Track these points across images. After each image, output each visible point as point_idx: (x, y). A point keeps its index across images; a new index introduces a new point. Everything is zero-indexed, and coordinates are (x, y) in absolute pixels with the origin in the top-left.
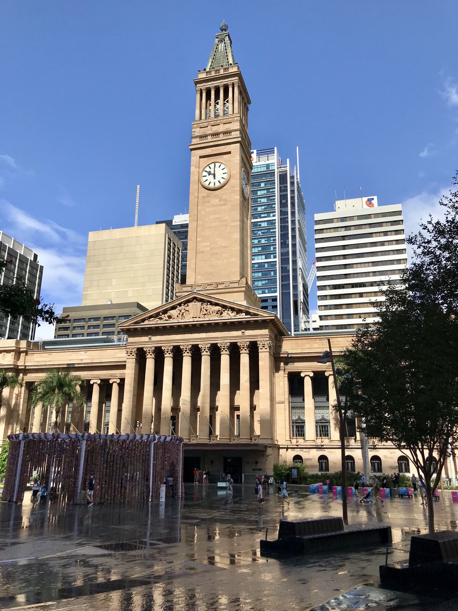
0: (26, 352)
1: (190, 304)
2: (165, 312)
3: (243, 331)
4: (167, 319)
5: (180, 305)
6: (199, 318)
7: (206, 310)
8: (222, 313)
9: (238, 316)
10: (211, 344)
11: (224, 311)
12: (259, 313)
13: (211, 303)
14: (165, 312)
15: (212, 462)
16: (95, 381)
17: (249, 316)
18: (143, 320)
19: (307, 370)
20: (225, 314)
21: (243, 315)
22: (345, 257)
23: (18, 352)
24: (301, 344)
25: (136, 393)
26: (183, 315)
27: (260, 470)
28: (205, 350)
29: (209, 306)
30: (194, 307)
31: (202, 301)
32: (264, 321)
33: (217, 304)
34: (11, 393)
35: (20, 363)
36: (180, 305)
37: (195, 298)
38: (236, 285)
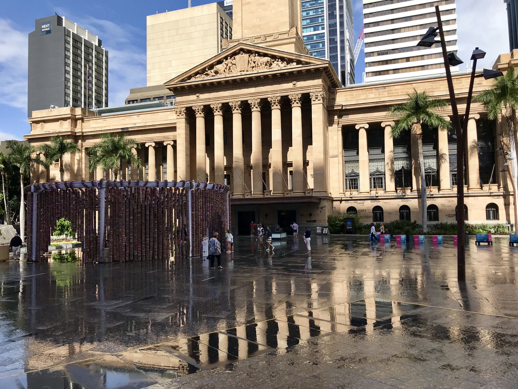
0: (82, 120)
2: (211, 67)
3: (294, 82)
4: (214, 74)
5: (226, 58)
6: (247, 71)
7: (254, 62)
8: (271, 64)
9: (289, 66)
10: (261, 99)
11: (273, 62)
12: (311, 61)
13: (260, 54)
14: (211, 67)
15: (266, 215)
16: (150, 144)
17: (301, 66)
18: (190, 78)
19: (361, 122)
20: (274, 65)
21: (294, 65)
22: (393, 21)
23: (74, 120)
24: (356, 95)
25: (189, 153)
26: (230, 69)
27: (315, 221)
28: (254, 105)
29: (257, 58)
31: (249, 52)
32: (317, 70)
33: (265, 55)
34: (72, 159)
35: (78, 130)
36: (226, 58)
37: (242, 50)
38: (286, 36)
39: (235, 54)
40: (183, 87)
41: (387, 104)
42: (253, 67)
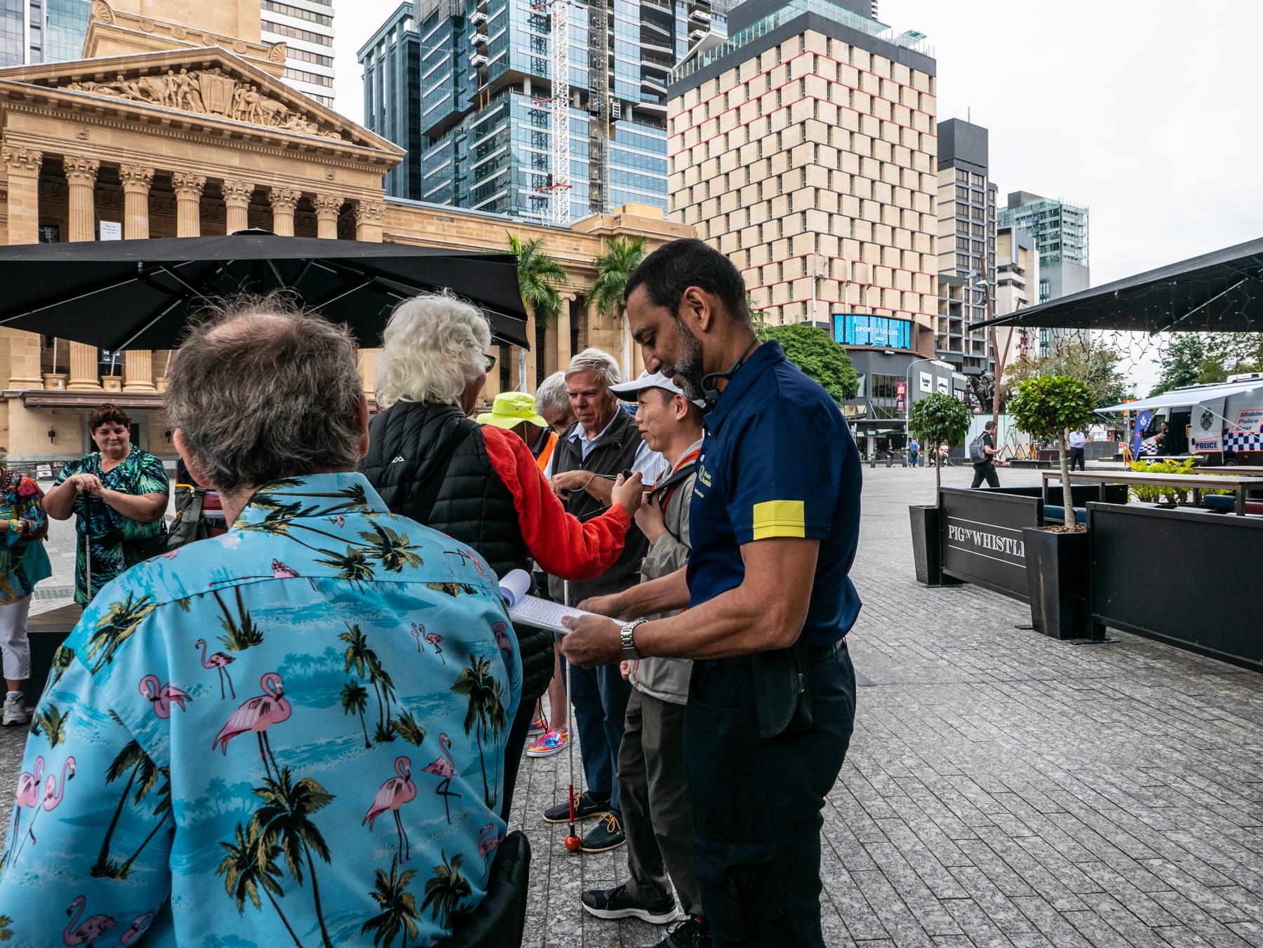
1: (205, 77)
2: (133, 75)
4: (139, 95)
5: (176, 69)
8: (285, 120)
14: (133, 75)
17: (350, 144)
18: (65, 81)
21: (337, 139)
26: (184, 97)
29: (254, 96)
30: (215, 87)
31: (233, 74)
33: (272, 96)
36: (176, 69)
37: (215, 65)
39: (196, 67)
40: (43, 101)
42: (244, 112)
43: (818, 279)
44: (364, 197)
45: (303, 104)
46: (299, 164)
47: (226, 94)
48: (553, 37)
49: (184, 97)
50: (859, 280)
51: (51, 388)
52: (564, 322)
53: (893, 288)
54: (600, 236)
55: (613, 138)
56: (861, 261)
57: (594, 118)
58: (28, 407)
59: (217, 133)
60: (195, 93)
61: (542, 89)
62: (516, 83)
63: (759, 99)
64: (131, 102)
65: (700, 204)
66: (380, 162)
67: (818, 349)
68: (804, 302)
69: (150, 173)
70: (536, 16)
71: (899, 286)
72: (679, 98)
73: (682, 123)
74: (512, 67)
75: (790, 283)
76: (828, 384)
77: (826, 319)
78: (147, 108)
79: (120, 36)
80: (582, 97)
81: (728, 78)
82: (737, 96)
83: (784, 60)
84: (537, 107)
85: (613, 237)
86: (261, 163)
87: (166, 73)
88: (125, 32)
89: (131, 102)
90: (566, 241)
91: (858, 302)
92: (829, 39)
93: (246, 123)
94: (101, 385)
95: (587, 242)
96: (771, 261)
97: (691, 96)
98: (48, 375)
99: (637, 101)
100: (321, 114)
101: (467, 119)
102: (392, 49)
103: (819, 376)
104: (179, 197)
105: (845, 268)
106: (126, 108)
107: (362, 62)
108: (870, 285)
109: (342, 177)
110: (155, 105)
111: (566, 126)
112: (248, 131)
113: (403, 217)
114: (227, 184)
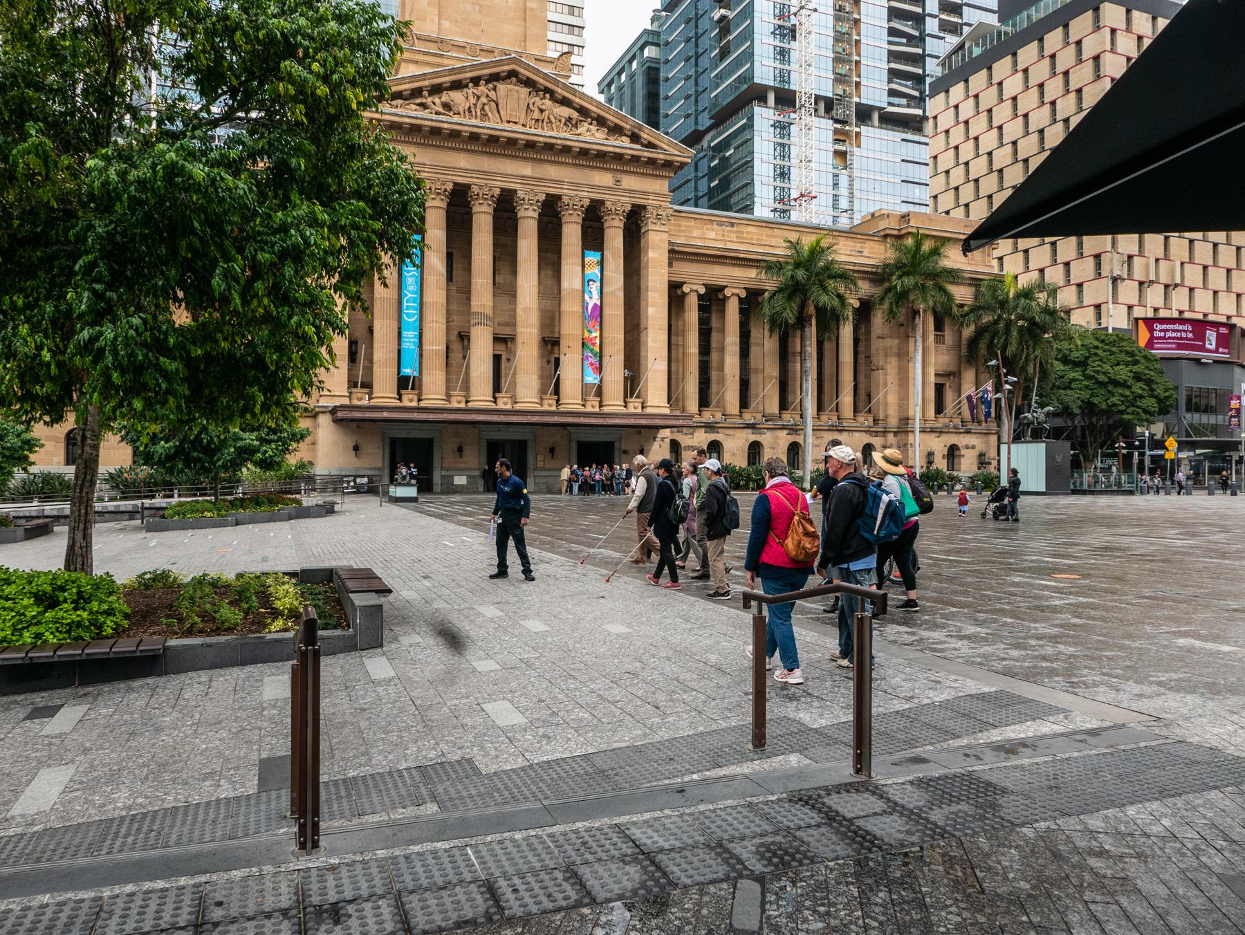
1: (502, 87)
2: (436, 90)
4: (441, 110)
5: (476, 81)
7: (542, 111)
13: (553, 98)
14: (436, 90)
15: (552, 451)
17: (639, 147)
20: (583, 128)
26: (483, 109)
29: (548, 103)
30: (512, 96)
31: (529, 83)
33: (565, 102)
36: (476, 81)
37: (512, 74)
39: (495, 78)
41: (741, 256)
43: (1115, 280)
44: (651, 202)
45: (594, 109)
46: (587, 172)
47: (521, 103)
48: (796, 48)
49: (483, 109)
50: (1164, 279)
51: (356, 402)
52: (846, 332)
53: (1205, 287)
54: (886, 236)
55: (859, 146)
56: (1166, 257)
57: (838, 126)
58: (337, 421)
59: (512, 142)
60: (493, 104)
61: (786, 99)
62: (758, 94)
63: (1041, 86)
64: (434, 117)
65: (967, 205)
66: (668, 164)
67: (1123, 357)
68: (1098, 307)
69: (450, 187)
70: (780, 27)
71: (1212, 285)
72: (943, 94)
73: (946, 120)
74: (756, 80)
75: (1080, 285)
76: (1141, 397)
77: (1123, 324)
78: (449, 122)
79: (420, 57)
80: (828, 105)
81: (1002, 67)
82: (1013, 85)
83: (1072, 39)
84: (780, 118)
85: (900, 237)
86: (552, 172)
87: (466, 86)
88: (425, 53)
89: (434, 117)
90: (850, 243)
91: (1161, 304)
92: (1128, 11)
93: (539, 131)
94: (400, 399)
95: (872, 244)
96: (1054, 262)
97: (957, 91)
98: (354, 390)
99: (885, 105)
100: (611, 118)
101: (708, 137)
102: (632, 76)
103: (1129, 387)
104: (474, 210)
105: (1147, 267)
106: (429, 123)
107: (602, 92)
108: (1176, 285)
109: (629, 182)
110: (456, 119)
111: (813, 136)
112: (541, 139)
113: (684, 223)
114: (520, 194)
